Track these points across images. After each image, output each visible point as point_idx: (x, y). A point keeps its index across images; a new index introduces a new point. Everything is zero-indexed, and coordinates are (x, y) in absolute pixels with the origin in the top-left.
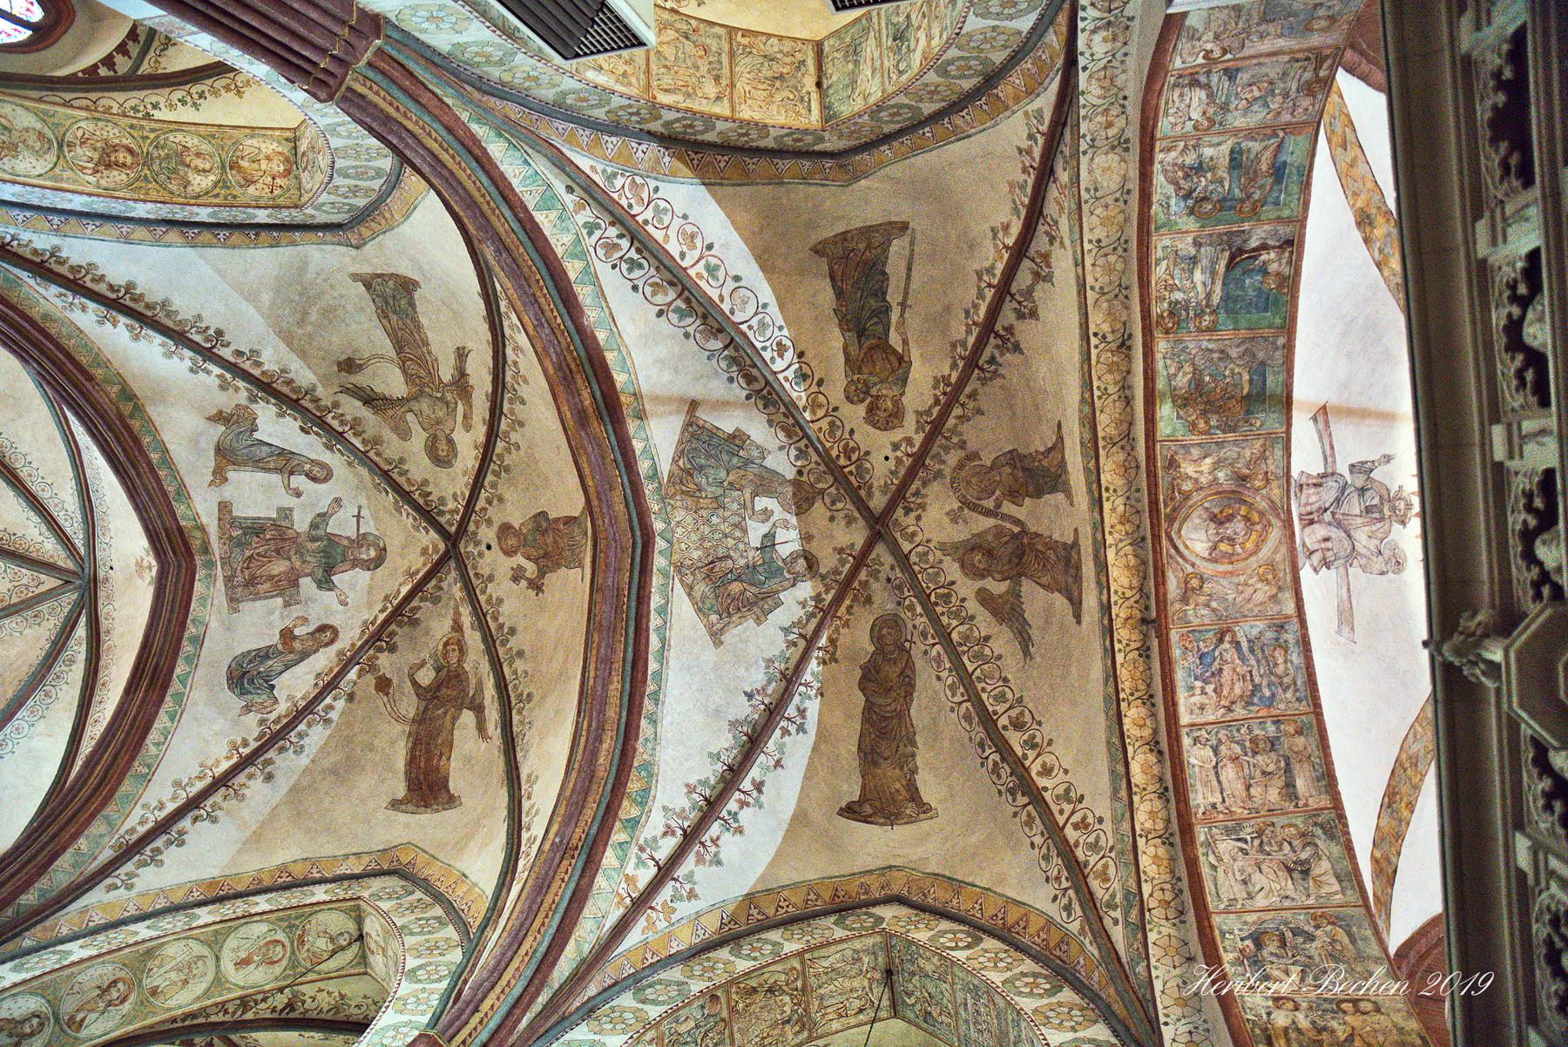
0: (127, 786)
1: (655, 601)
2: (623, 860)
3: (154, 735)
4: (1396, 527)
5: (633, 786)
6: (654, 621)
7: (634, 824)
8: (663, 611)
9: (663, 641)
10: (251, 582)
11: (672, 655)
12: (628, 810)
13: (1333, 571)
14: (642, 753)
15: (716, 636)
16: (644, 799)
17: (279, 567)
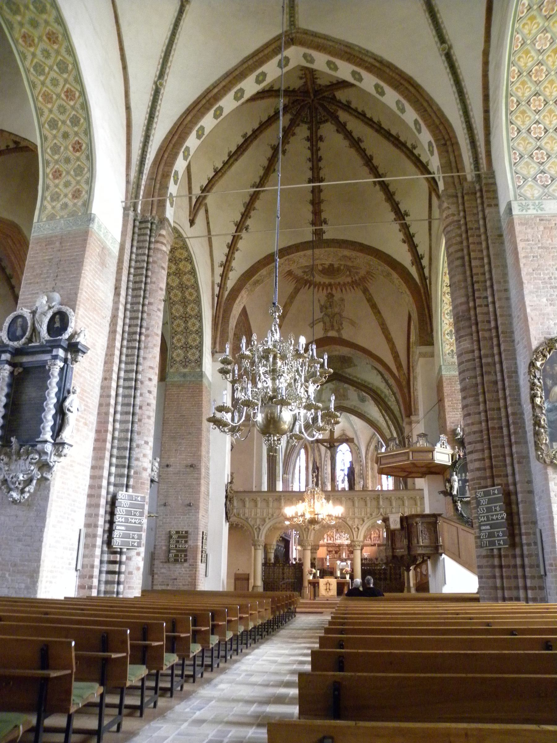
0: (379, 425)
1: (347, 376)
2: (390, 401)
3: (371, 418)
4: (335, 298)
5: (379, 392)
6: (351, 377)
7: (386, 396)
8: (349, 375)
9: (356, 377)
10: (344, 396)
11: (358, 376)
12: (383, 396)
13: (344, 323)
14: (374, 388)
15: (355, 365)
16: (382, 392)
17: (341, 391)
